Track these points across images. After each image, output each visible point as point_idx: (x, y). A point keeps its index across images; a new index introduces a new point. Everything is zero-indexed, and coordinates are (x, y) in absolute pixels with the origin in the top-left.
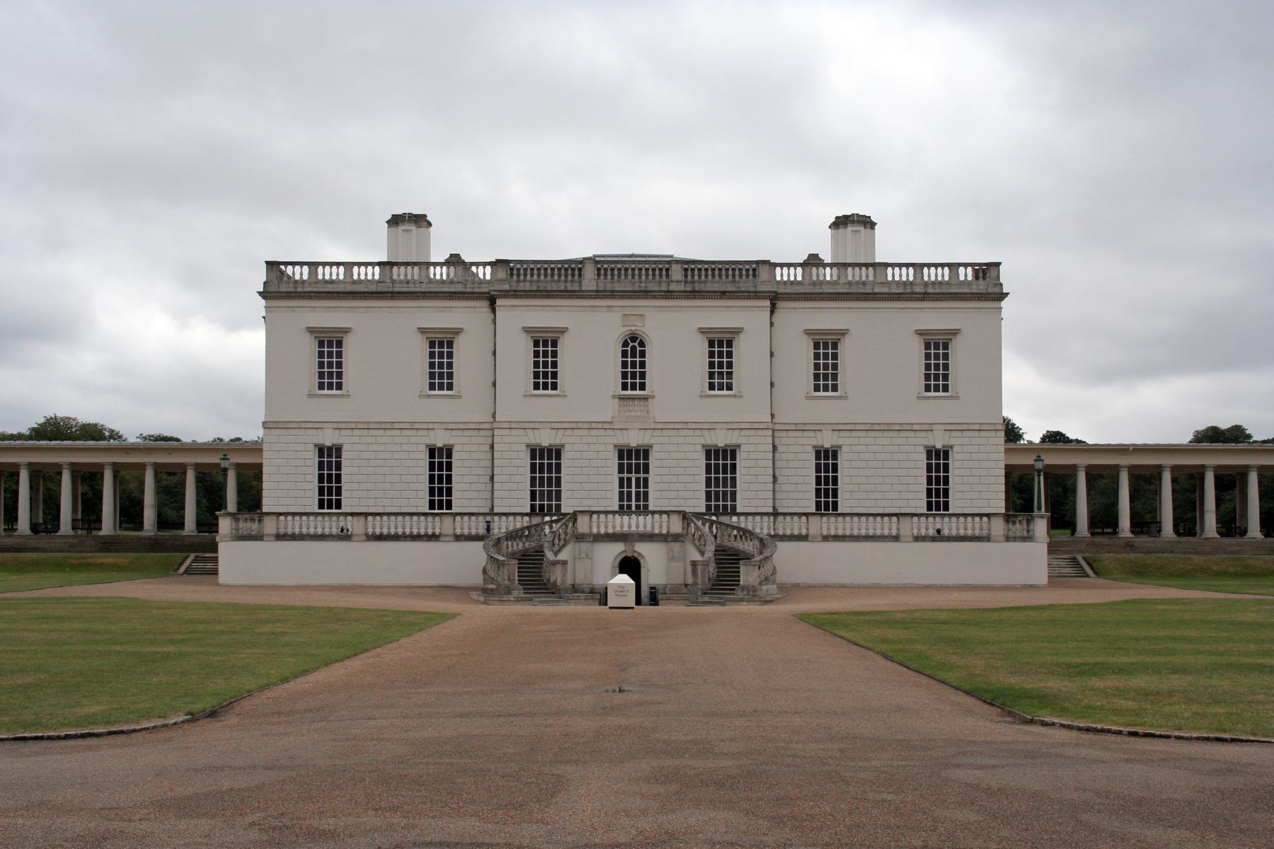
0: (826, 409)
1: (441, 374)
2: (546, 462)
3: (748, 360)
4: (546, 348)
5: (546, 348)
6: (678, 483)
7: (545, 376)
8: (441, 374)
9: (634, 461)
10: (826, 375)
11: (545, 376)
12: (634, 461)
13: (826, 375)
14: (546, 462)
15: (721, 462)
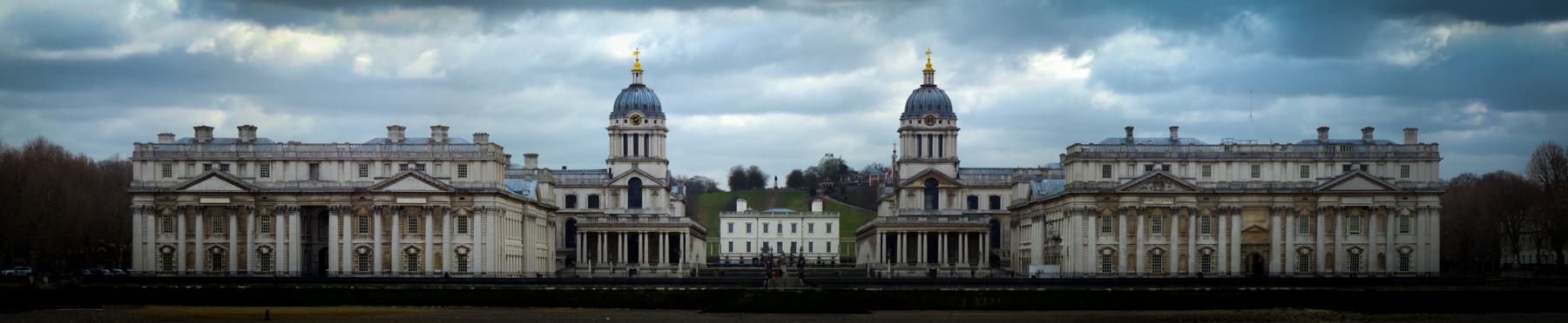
0: (811, 236)
1: (749, 230)
2: (766, 244)
3: (798, 228)
4: (766, 226)
5: (766, 226)
6: (787, 249)
7: (766, 230)
8: (749, 230)
9: (780, 244)
10: (811, 230)
11: (766, 230)
12: (780, 244)
13: (811, 230)
14: (766, 244)
15: (794, 244)
